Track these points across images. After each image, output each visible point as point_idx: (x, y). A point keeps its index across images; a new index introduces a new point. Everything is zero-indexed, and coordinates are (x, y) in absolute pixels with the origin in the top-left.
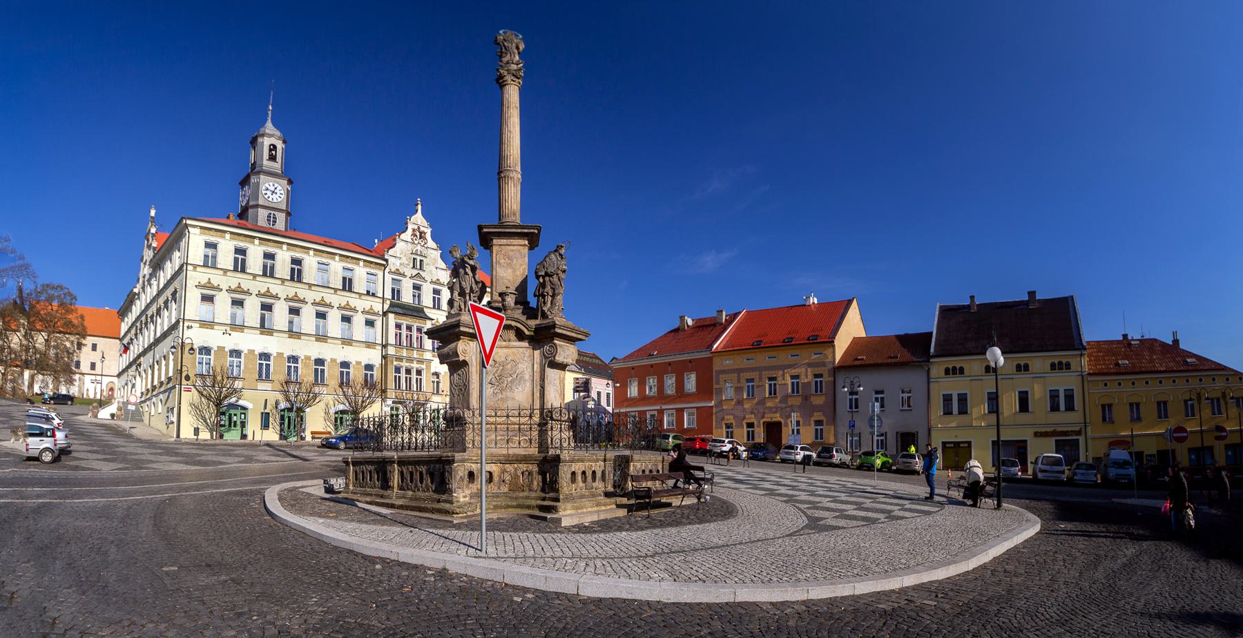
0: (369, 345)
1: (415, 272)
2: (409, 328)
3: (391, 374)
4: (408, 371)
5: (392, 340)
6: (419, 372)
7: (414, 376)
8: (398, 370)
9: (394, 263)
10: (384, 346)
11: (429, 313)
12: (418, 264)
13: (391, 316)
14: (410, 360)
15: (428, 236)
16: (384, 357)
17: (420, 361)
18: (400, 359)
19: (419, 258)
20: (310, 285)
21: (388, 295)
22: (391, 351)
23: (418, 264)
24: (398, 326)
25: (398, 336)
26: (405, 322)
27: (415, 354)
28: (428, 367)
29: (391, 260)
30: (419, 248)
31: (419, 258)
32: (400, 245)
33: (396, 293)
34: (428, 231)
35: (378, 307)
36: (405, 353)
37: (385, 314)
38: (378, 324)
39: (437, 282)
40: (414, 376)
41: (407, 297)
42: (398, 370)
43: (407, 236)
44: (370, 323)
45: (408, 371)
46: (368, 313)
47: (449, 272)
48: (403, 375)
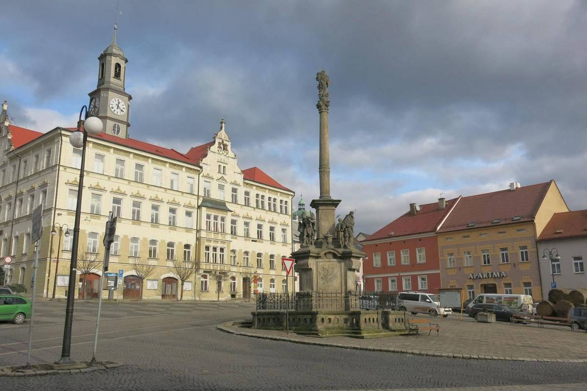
0: (188, 230)
1: (220, 176)
2: (216, 218)
3: (203, 251)
4: (215, 249)
5: (204, 227)
6: (222, 250)
7: (218, 252)
8: (207, 248)
9: (206, 170)
10: (198, 231)
11: (229, 206)
12: (222, 170)
13: (204, 209)
14: (216, 241)
15: (229, 148)
16: (198, 239)
17: (223, 242)
18: (209, 240)
19: (222, 165)
20: (148, 185)
21: (202, 193)
22: (203, 234)
23: (222, 170)
24: (208, 217)
25: (208, 224)
26: (213, 213)
27: (220, 237)
28: (229, 246)
29: (204, 167)
30: (223, 157)
31: (222, 165)
32: (210, 154)
33: (207, 191)
34: (229, 144)
35: (194, 202)
36: (212, 236)
37: (199, 207)
38: (194, 215)
39: (235, 183)
40: (218, 252)
41: (216, 195)
42: (207, 248)
43: (214, 148)
44: (189, 214)
45: (215, 249)
46: (188, 207)
47: (243, 175)
48: (211, 251)
